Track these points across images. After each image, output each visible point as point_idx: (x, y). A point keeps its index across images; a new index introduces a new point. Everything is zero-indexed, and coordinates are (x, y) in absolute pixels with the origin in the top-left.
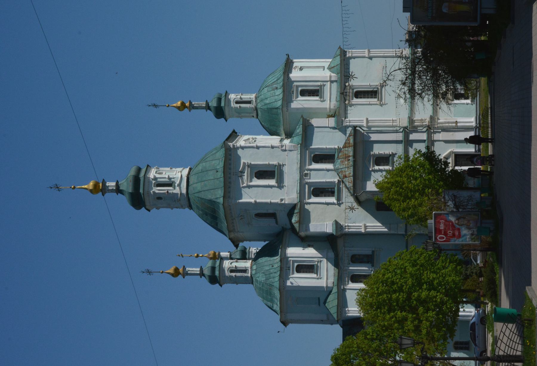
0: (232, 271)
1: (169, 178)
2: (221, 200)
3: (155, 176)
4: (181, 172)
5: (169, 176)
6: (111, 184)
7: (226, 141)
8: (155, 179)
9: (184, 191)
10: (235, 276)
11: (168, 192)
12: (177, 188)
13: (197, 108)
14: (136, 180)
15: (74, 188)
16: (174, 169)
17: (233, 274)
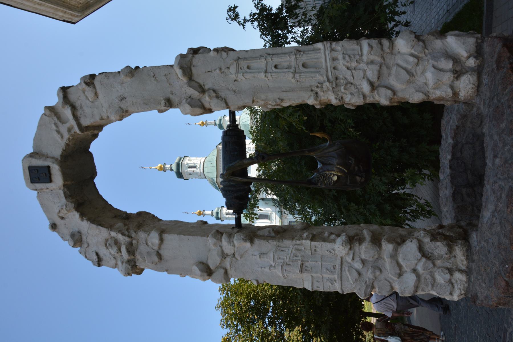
0: (227, 214)
1: (194, 164)
2: (215, 179)
3: (187, 163)
4: (201, 160)
5: (194, 163)
6: (168, 166)
7: (218, 146)
8: (187, 164)
9: (202, 171)
10: (229, 217)
11: (193, 171)
12: (198, 169)
13: (209, 125)
14: (178, 165)
15: (151, 168)
16: (198, 158)
17: (228, 216)
